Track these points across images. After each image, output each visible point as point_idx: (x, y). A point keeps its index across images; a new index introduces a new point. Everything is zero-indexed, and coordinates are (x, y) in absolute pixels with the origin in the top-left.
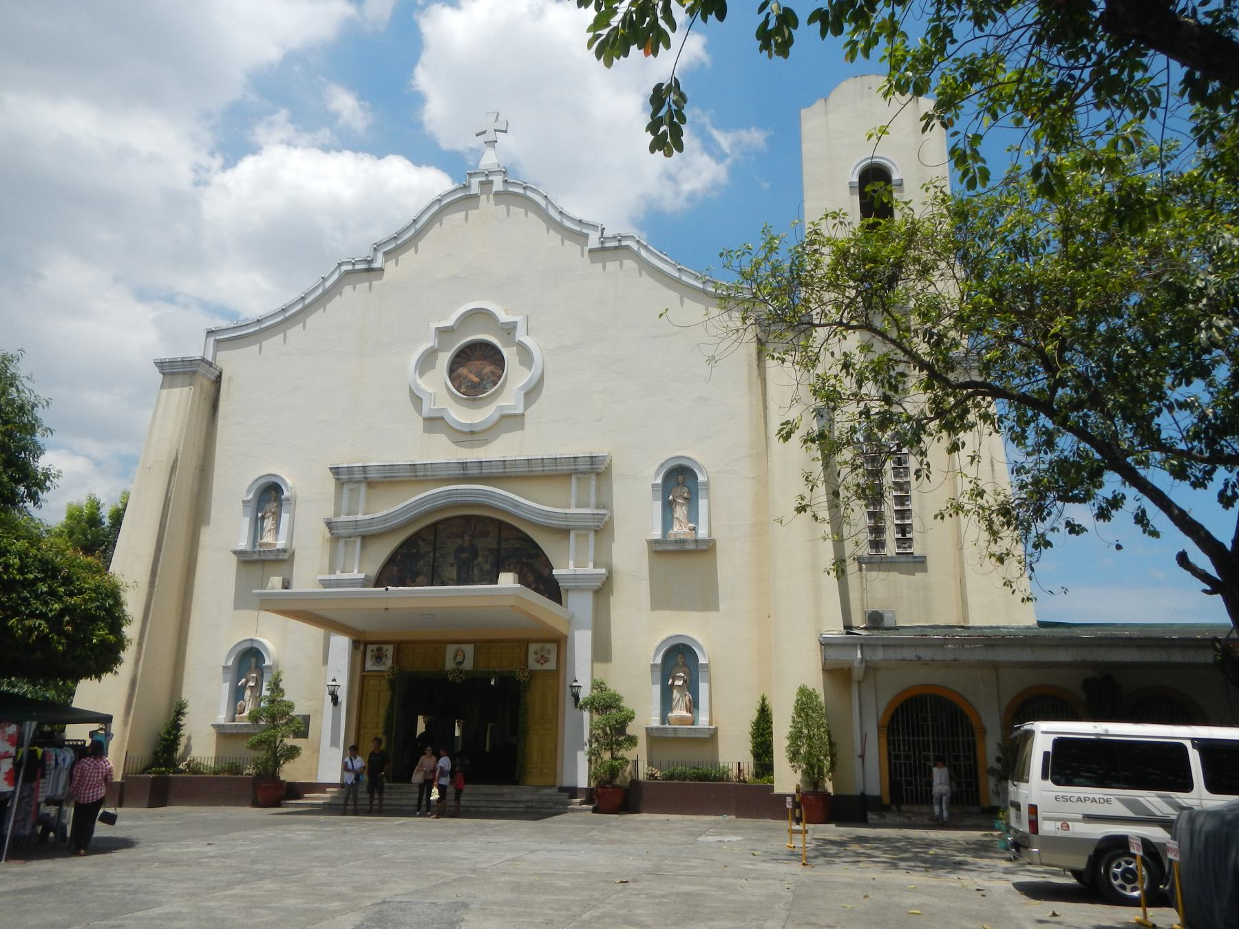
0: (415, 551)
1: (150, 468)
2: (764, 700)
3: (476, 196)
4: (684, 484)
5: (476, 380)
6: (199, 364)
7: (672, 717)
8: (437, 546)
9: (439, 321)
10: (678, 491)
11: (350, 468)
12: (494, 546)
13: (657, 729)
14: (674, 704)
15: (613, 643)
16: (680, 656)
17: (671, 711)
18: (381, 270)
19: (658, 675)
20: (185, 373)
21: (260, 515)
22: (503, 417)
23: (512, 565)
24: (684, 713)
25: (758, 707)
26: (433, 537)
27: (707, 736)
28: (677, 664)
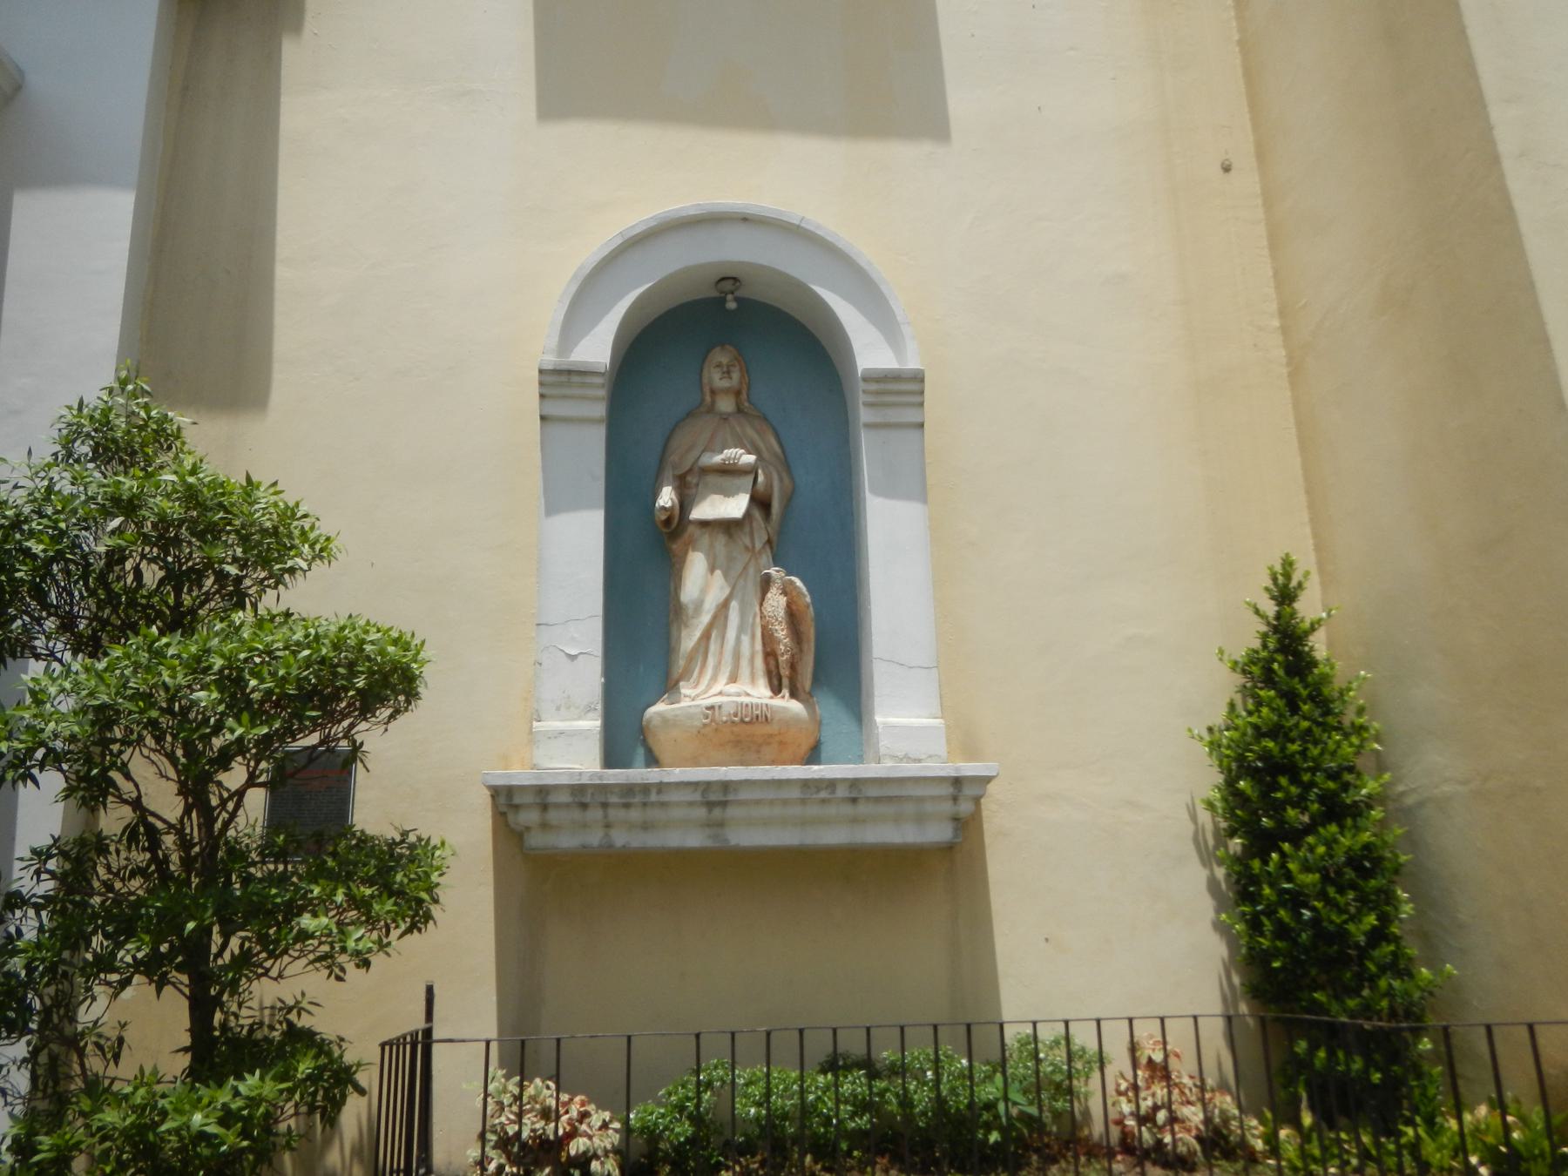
2: (1285, 595)
7: (665, 720)
13: (582, 795)
14: (689, 640)
15: (283, 274)
16: (721, 356)
17: (668, 687)
19: (592, 444)
24: (759, 693)
25: (1248, 636)
27: (939, 833)
28: (701, 409)
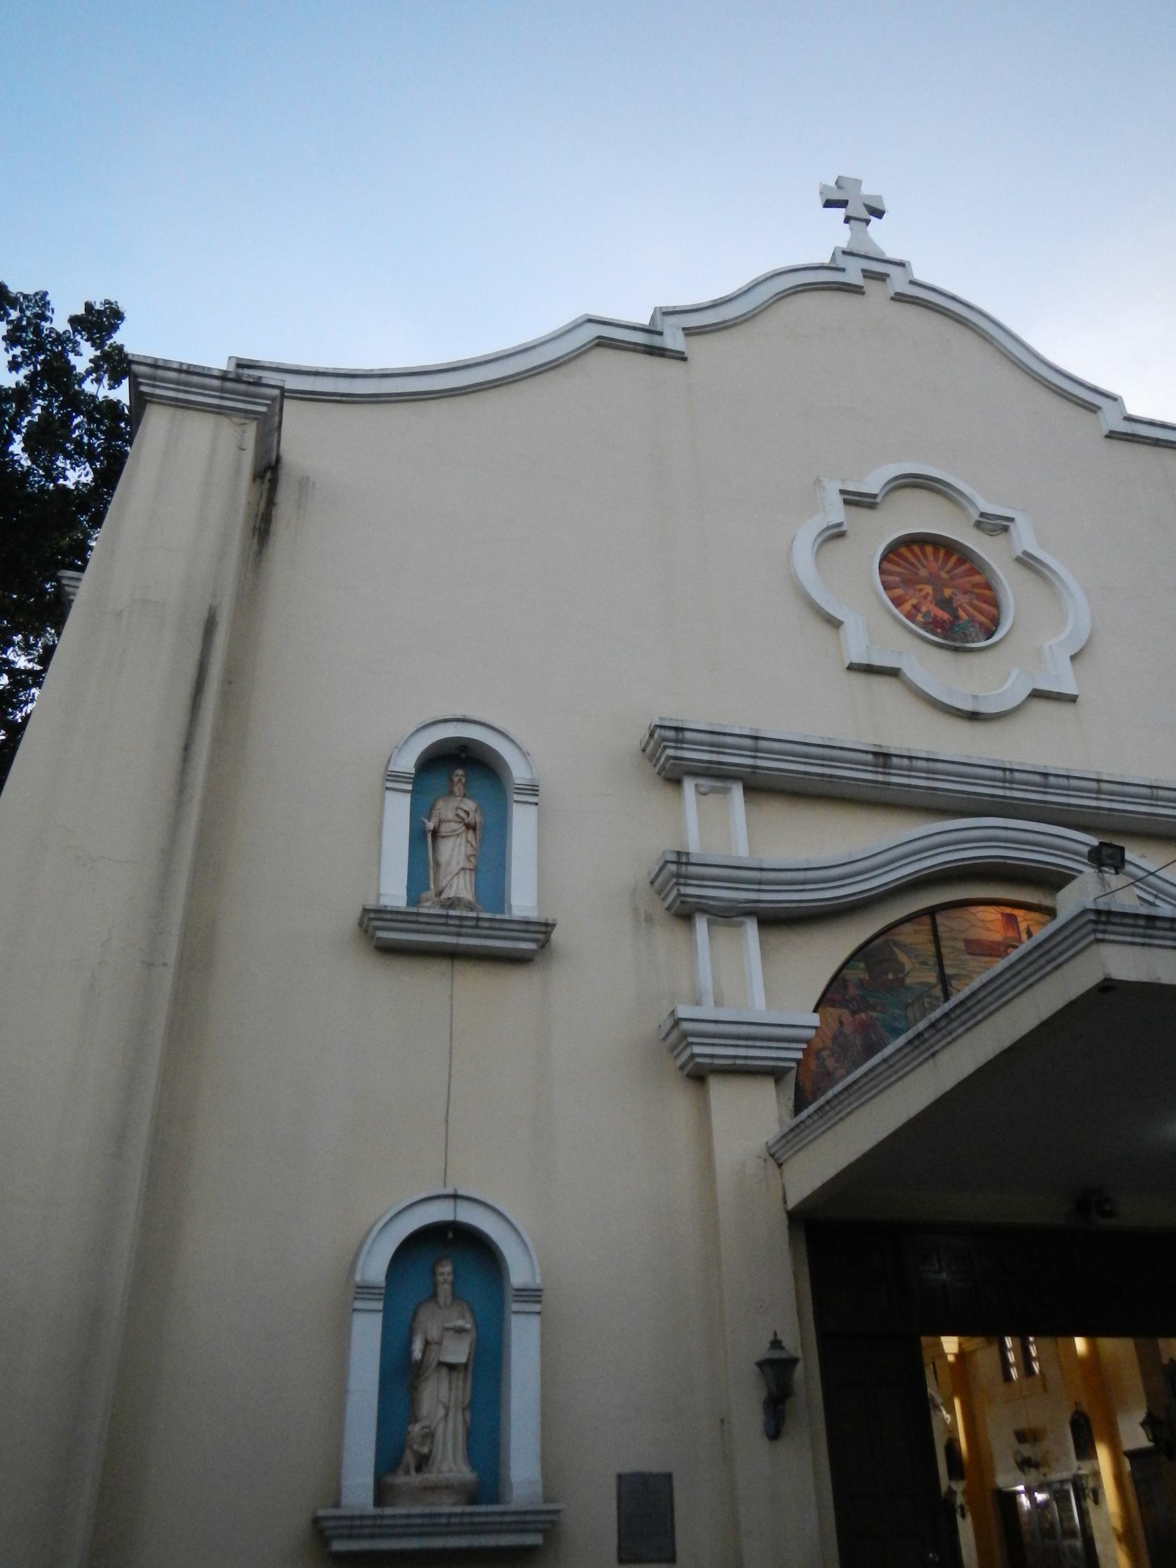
0: (890, 976)
1: (119, 614)
5: (945, 616)
6: (273, 399)
8: (949, 971)
9: (844, 481)
11: (716, 739)
18: (681, 357)
20: (219, 411)
21: (431, 825)
22: (1037, 694)
26: (931, 948)
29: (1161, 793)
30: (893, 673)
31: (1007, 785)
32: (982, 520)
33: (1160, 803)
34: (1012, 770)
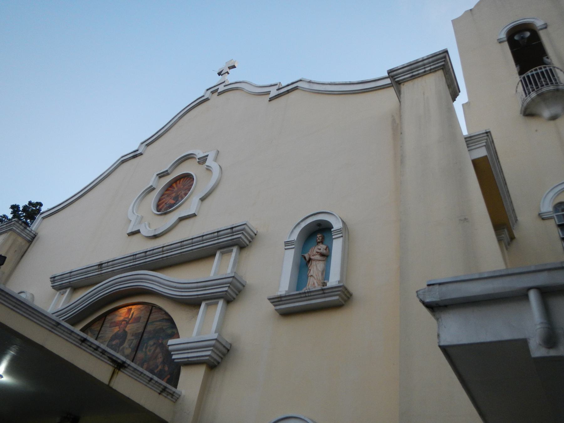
3: (207, 99)
4: (322, 242)
6: (14, 224)
10: (316, 250)
12: (141, 331)
18: (141, 154)
22: (181, 219)
23: (148, 348)
29: (185, 243)
30: (138, 232)
31: (134, 261)
32: (199, 160)
33: (184, 247)
34: (136, 255)
